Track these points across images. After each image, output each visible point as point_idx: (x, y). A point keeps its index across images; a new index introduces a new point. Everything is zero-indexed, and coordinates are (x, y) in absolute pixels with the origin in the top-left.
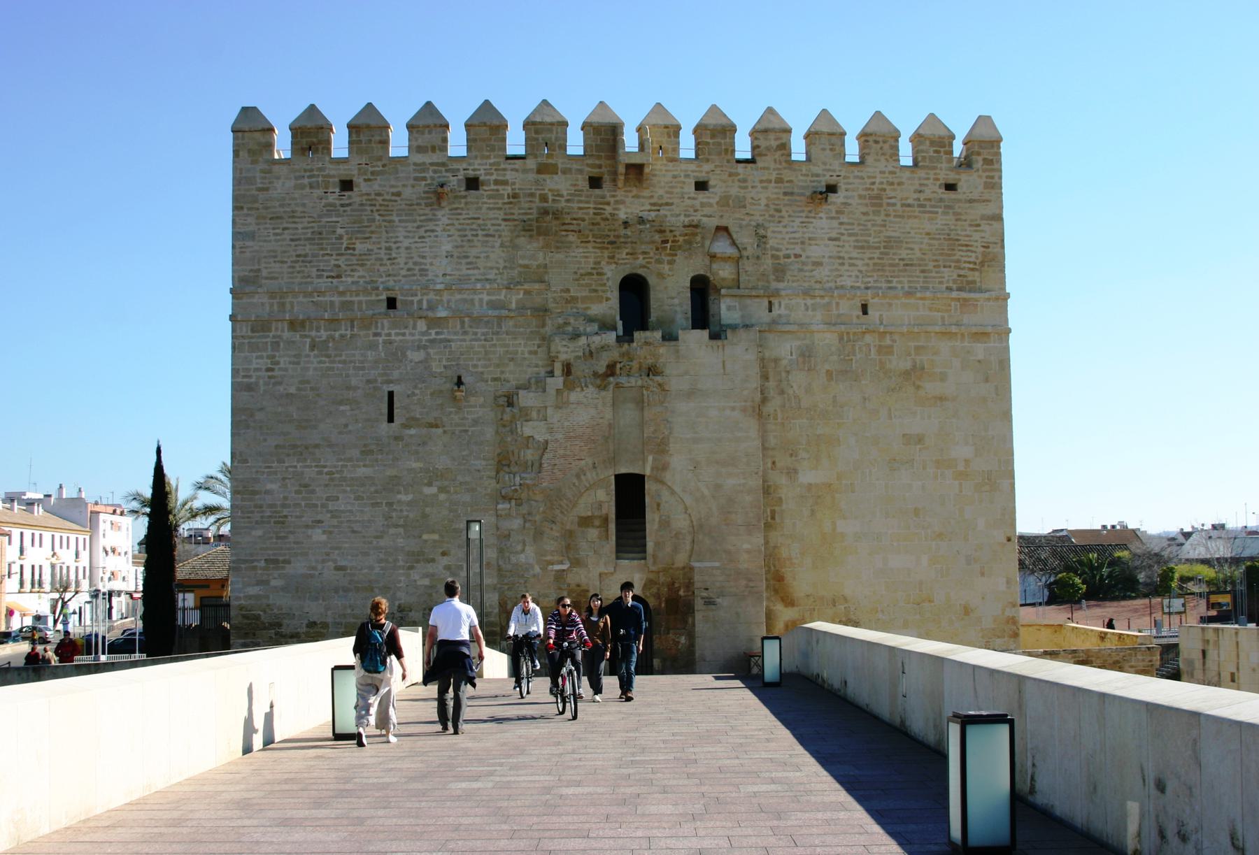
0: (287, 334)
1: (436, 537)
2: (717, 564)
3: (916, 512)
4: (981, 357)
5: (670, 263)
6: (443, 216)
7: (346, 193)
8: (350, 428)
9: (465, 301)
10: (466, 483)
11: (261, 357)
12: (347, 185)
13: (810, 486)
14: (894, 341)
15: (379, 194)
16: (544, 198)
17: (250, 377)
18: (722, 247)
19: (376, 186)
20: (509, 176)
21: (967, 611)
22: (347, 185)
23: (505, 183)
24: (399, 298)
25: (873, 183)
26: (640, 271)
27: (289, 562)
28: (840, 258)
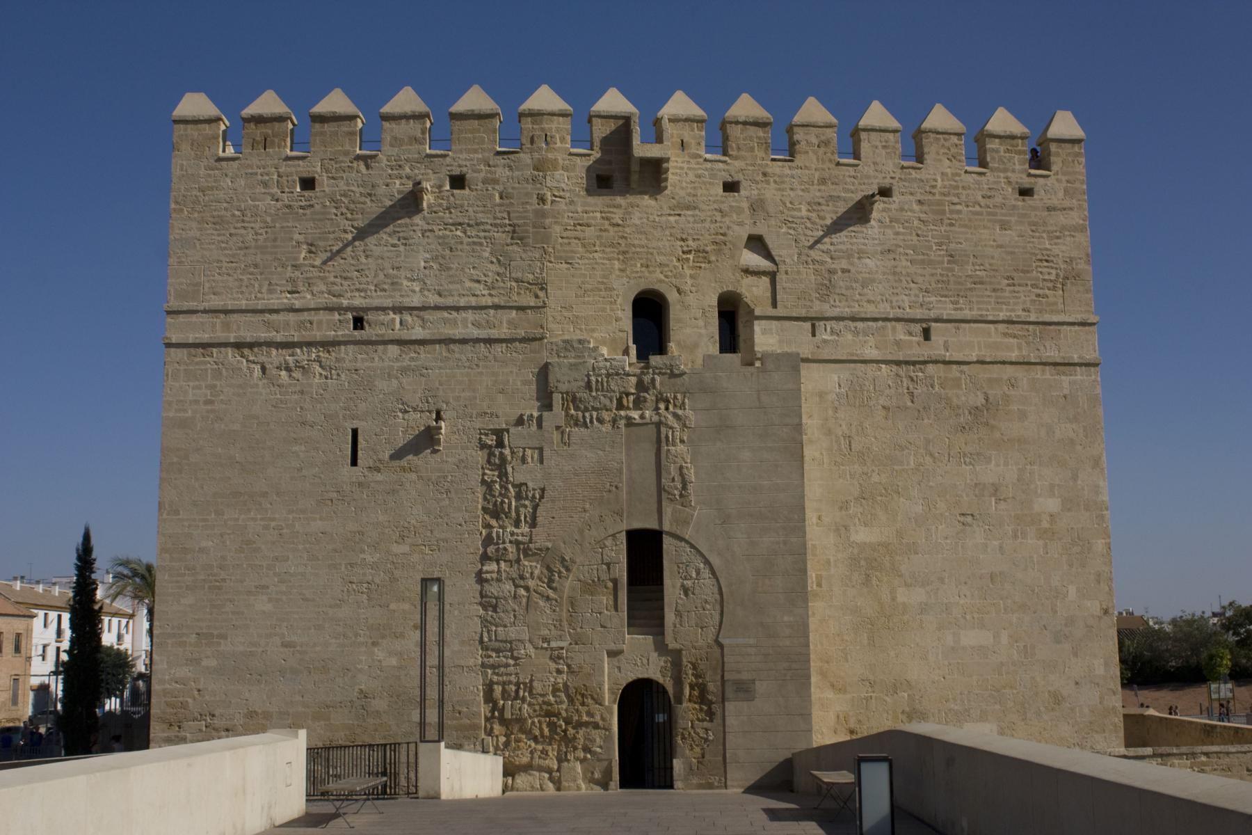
2: (752, 641)
3: (992, 577)
4: (1066, 392)
5: (691, 276)
7: (306, 193)
8: (304, 472)
9: (445, 321)
10: (445, 540)
11: (199, 388)
14: (962, 372)
15: (345, 195)
16: (542, 199)
17: (185, 411)
19: (342, 186)
20: (502, 172)
21: (1057, 699)
22: (308, 183)
23: (495, 181)
24: (370, 317)
25: (934, 187)
26: (656, 287)
27: (224, 637)
28: (894, 273)
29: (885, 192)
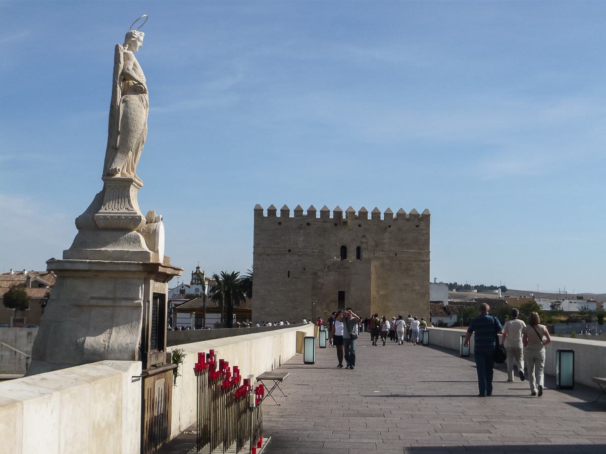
0: (266, 257)
1: (298, 303)
6: (302, 231)
12: (280, 224)
13: (382, 295)
16: (324, 228)
18: (364, 240)
22: (280, 224)
26: (345, 245)
29: (390, 227)
